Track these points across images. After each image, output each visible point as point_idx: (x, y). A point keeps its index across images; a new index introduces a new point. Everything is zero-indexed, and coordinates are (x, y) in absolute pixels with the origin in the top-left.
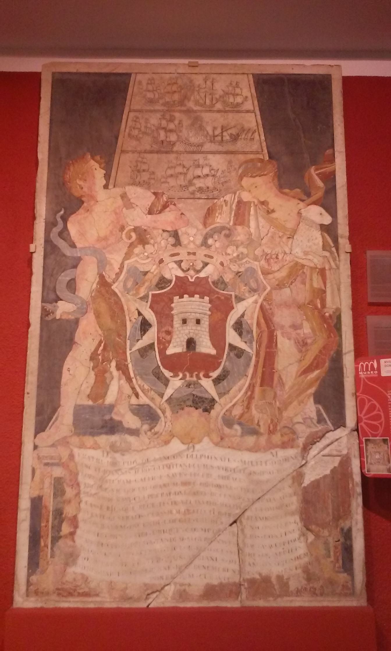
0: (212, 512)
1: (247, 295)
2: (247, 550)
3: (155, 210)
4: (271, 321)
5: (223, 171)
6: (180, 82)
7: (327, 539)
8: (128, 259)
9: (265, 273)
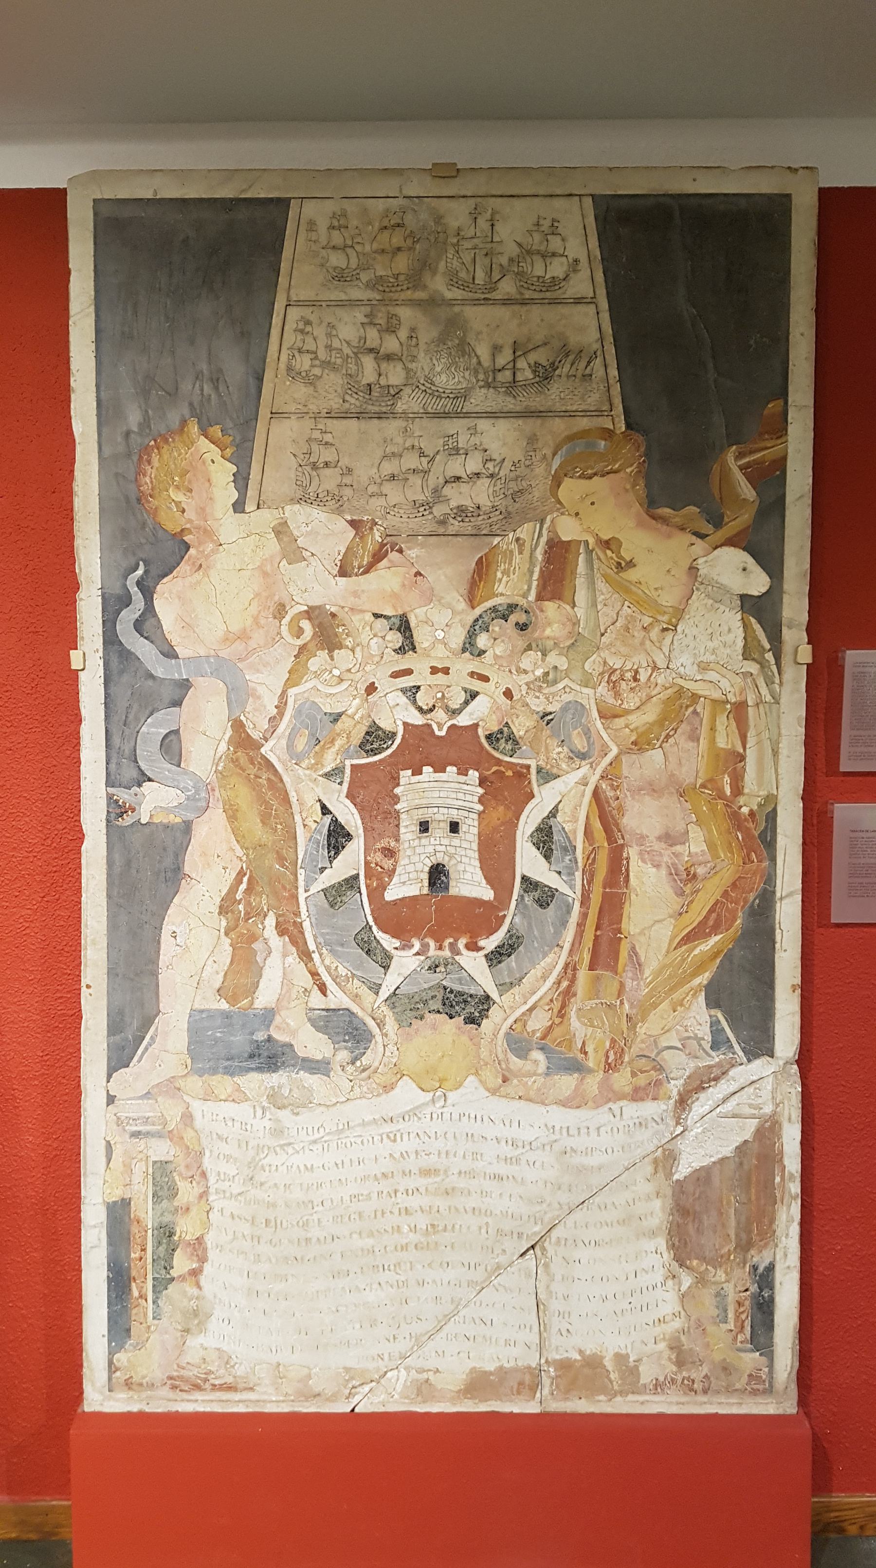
0: (483, 1231)
1: (564, 766)
2: (555, 1305)
3: (356, 564)
4: (617, 825)
5: (514, 465)
6: (409, 219)
7: (722, 1289)
8: (296, 684)
9: (607, 715)
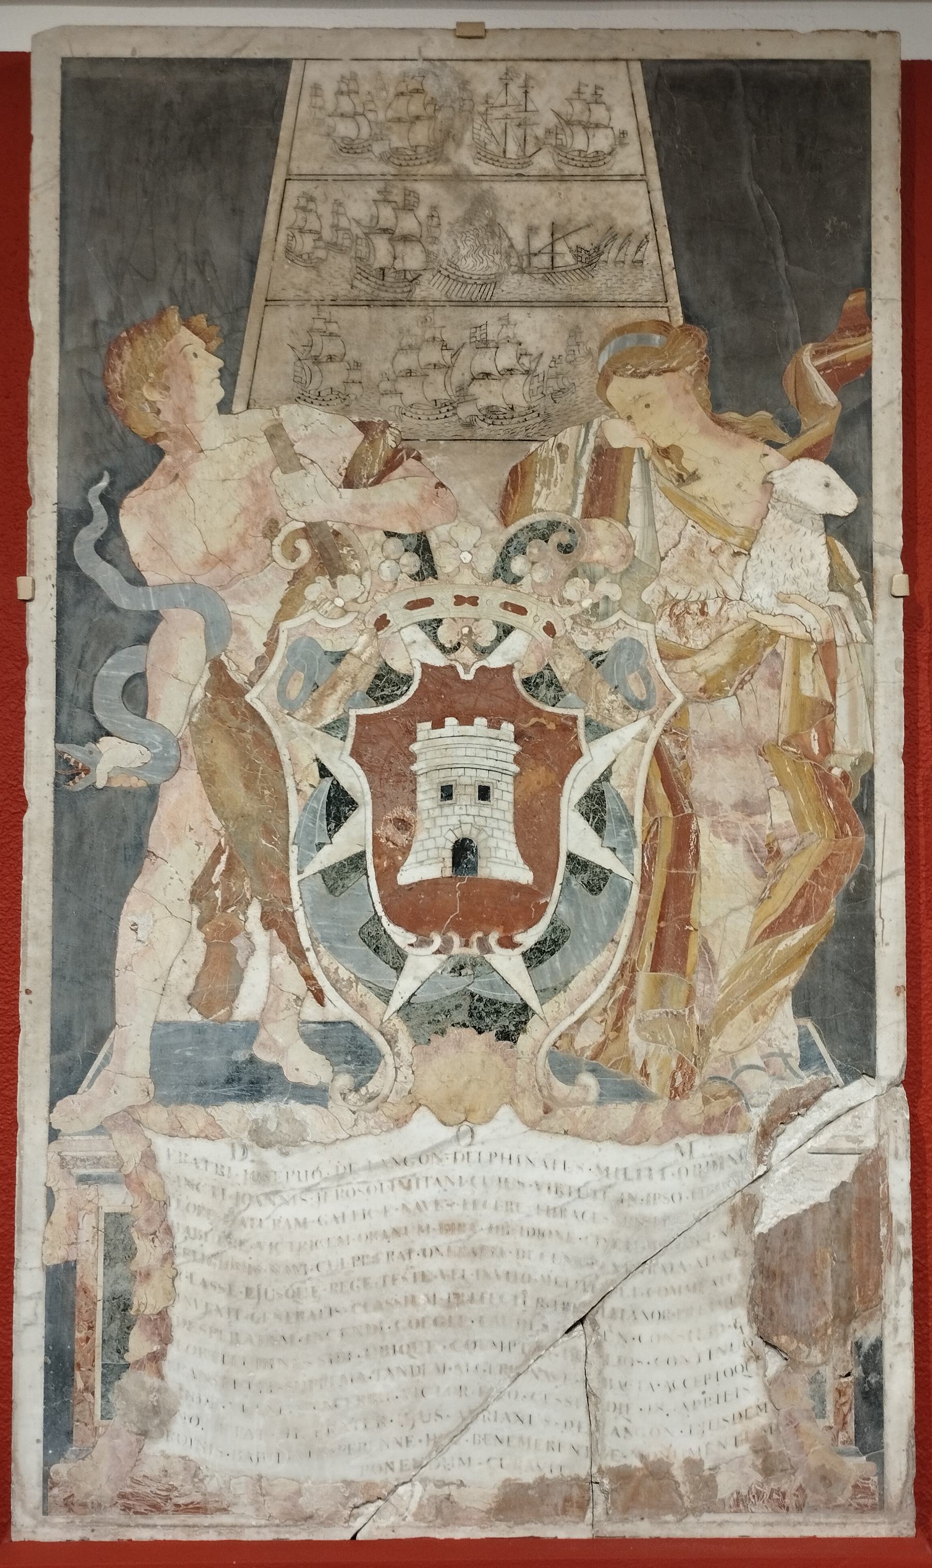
0: (520, 1301)
1: (618, 718)
2: (610, 1396)
4: (684, 790)
5: (554, 360)
6: (430, 85)
7: (818, 1373)
9: (671, 655)
